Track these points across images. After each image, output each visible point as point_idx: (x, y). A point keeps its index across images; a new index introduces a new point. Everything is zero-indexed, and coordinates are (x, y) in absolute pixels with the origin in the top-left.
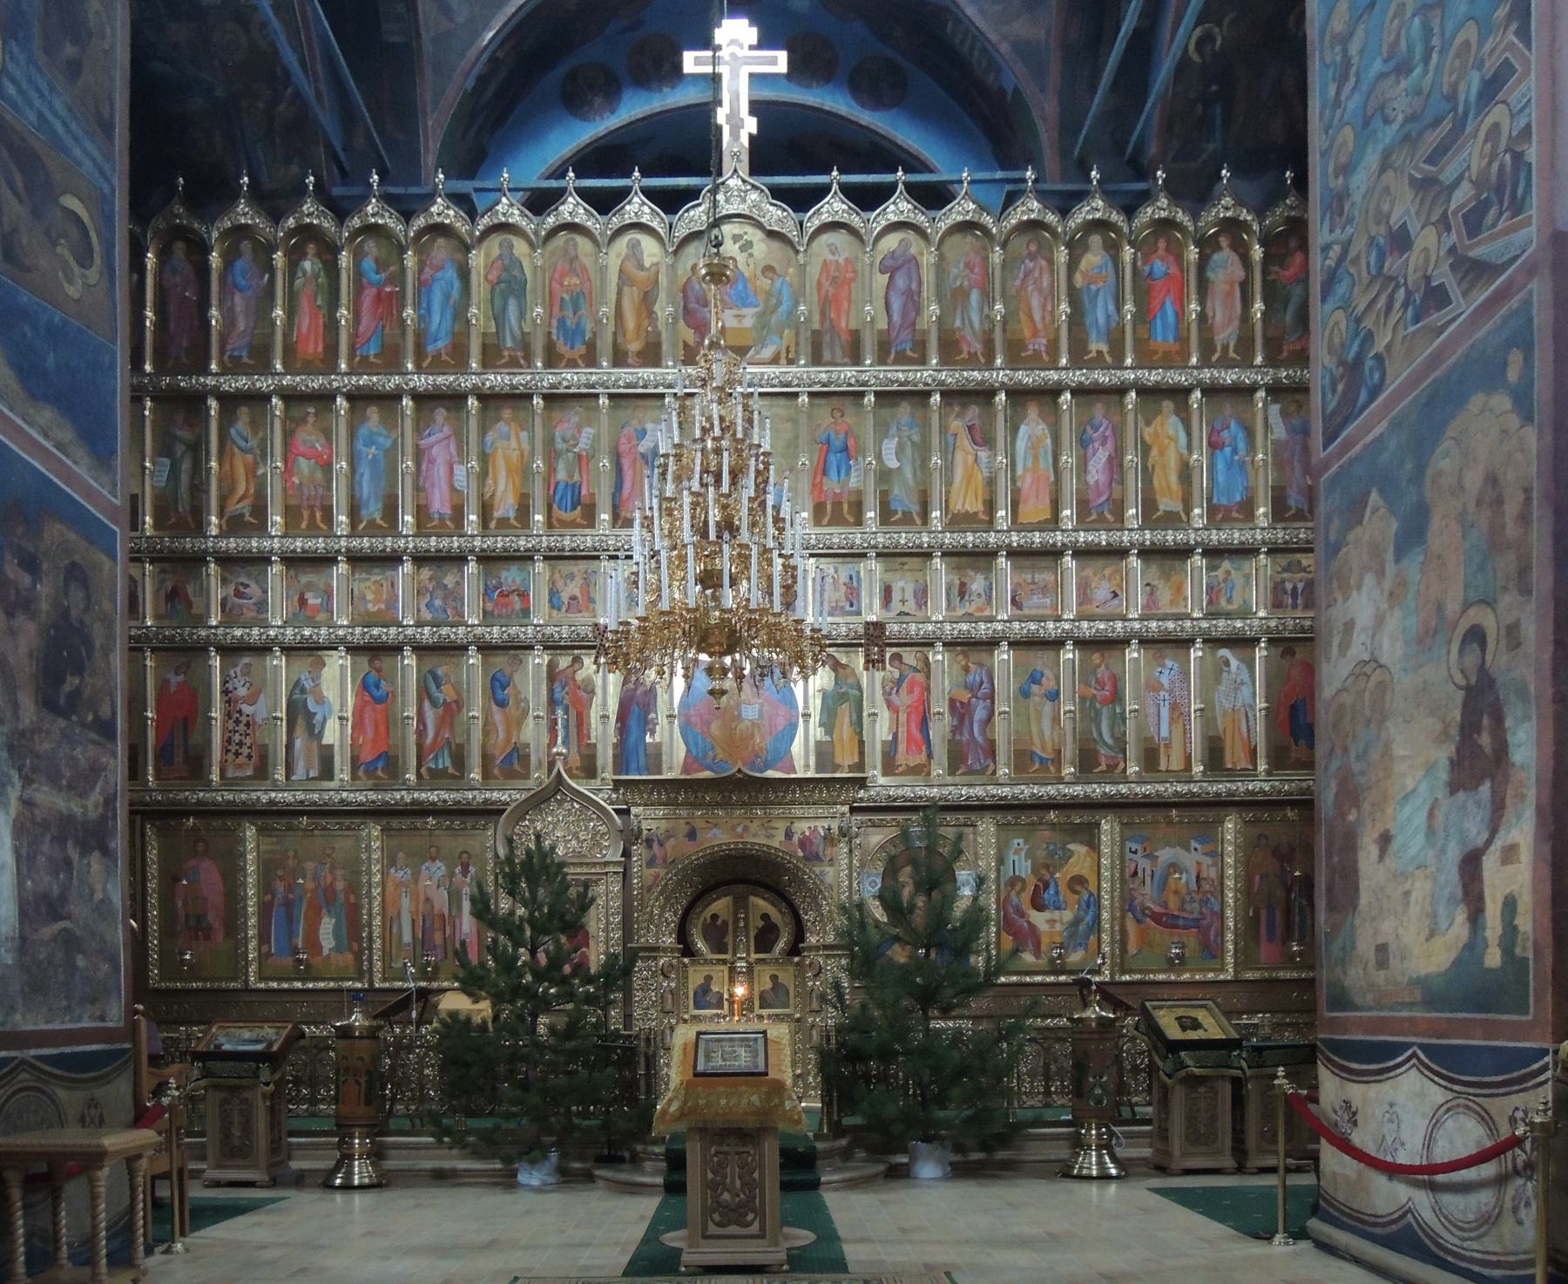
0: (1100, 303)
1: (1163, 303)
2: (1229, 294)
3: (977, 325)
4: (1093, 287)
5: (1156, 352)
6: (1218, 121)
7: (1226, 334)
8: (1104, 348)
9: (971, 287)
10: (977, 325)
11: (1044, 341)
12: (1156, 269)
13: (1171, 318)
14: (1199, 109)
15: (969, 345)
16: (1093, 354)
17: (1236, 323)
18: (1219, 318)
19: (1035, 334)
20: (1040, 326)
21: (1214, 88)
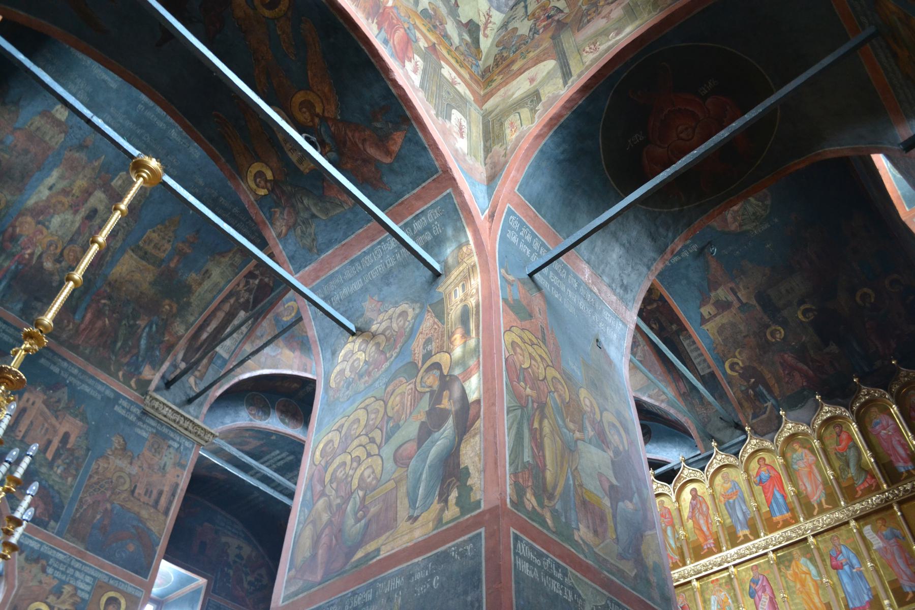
0: (737, 508)
1: (773, 493)
2: (810, 472)
3: (673, 546)
4: (731, 501)
5: (778, 523)
6: (765, 392)
7: (817, 496)
8: (747, 532)
9: (666, 526)
10: (673, 546)
11: (712, 541)
12: (762, 477)
13: (781, 500)
14: (751, 391)
15: (672, 558)
16: (742, 538)
17: (821, 487)
18: (809, 489)
19: (706, 540)
20: (707, 533)
21: (753, 380)
